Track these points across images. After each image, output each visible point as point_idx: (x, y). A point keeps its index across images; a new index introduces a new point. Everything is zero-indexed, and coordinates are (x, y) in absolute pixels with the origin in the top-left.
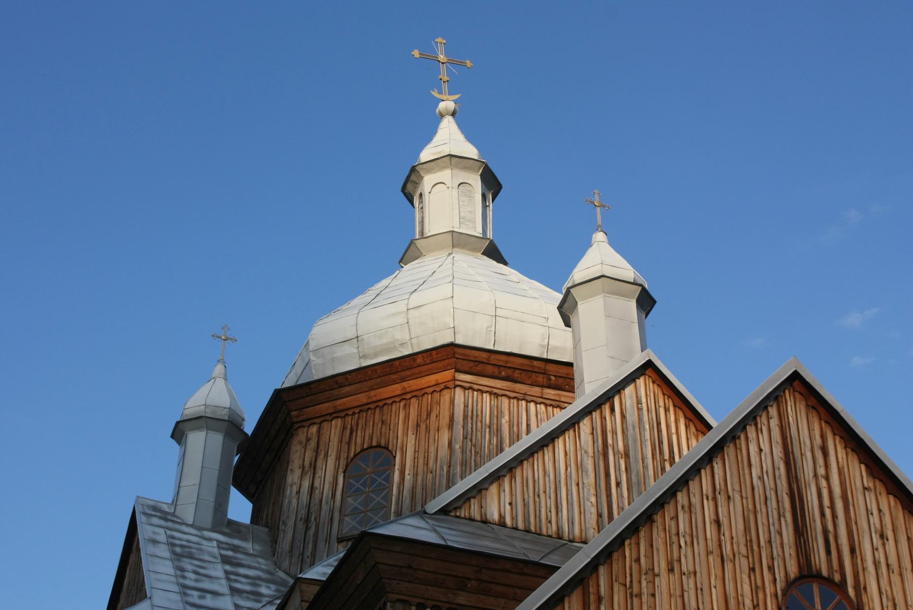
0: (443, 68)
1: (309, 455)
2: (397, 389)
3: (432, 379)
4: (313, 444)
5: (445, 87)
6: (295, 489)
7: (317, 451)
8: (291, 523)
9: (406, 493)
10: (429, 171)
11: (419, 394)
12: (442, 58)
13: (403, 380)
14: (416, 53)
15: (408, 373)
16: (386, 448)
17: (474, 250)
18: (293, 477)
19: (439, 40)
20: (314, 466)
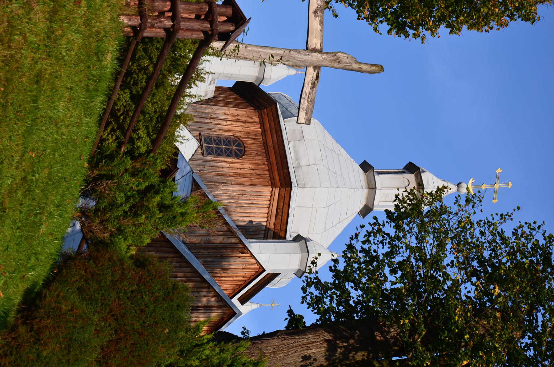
0: (490, 186)
1: (244, 119)
2: (273, 160)
3: (277, 178)
4: (249, 120)
6: (227, 112)
7: (245, 122)
8: (210, 111)
9: (220, 164)
11: (270, 170)
12: (497, 186)
13: (277, 163)
14: (499, 171)
16: (244, 155)
17: (367, 200)
18: (233, 111)
19: (510, 184)
20: (238, 120)
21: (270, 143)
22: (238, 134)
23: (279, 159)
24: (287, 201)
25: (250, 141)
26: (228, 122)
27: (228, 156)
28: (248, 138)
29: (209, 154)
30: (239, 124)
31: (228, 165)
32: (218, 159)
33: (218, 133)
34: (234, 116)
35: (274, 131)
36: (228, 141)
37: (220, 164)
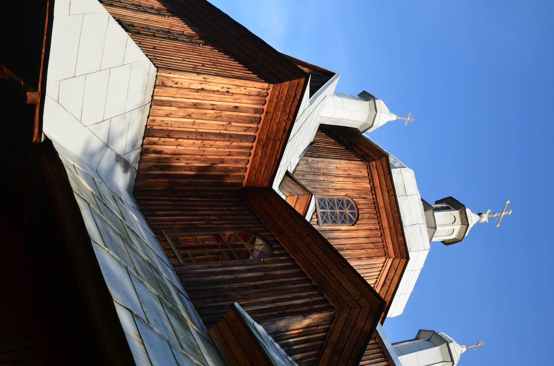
5: (491, 216)
10: (461, 213)
15: (394, 231)
21: (381, 204)
22: (350, 193)
23: (392, 223)
24: (399, 272)
25: (361, 201)
26: (340, 179)
27: (343, 222)
28: (360, 198)
29: (325, 222)
30: (349, 180)
31: (344, 235)
32: (334, 227)
33: (332, 193)
34: (345, 170)
35: (385, 188)
36: (341, 203)
37: (336, 234)
